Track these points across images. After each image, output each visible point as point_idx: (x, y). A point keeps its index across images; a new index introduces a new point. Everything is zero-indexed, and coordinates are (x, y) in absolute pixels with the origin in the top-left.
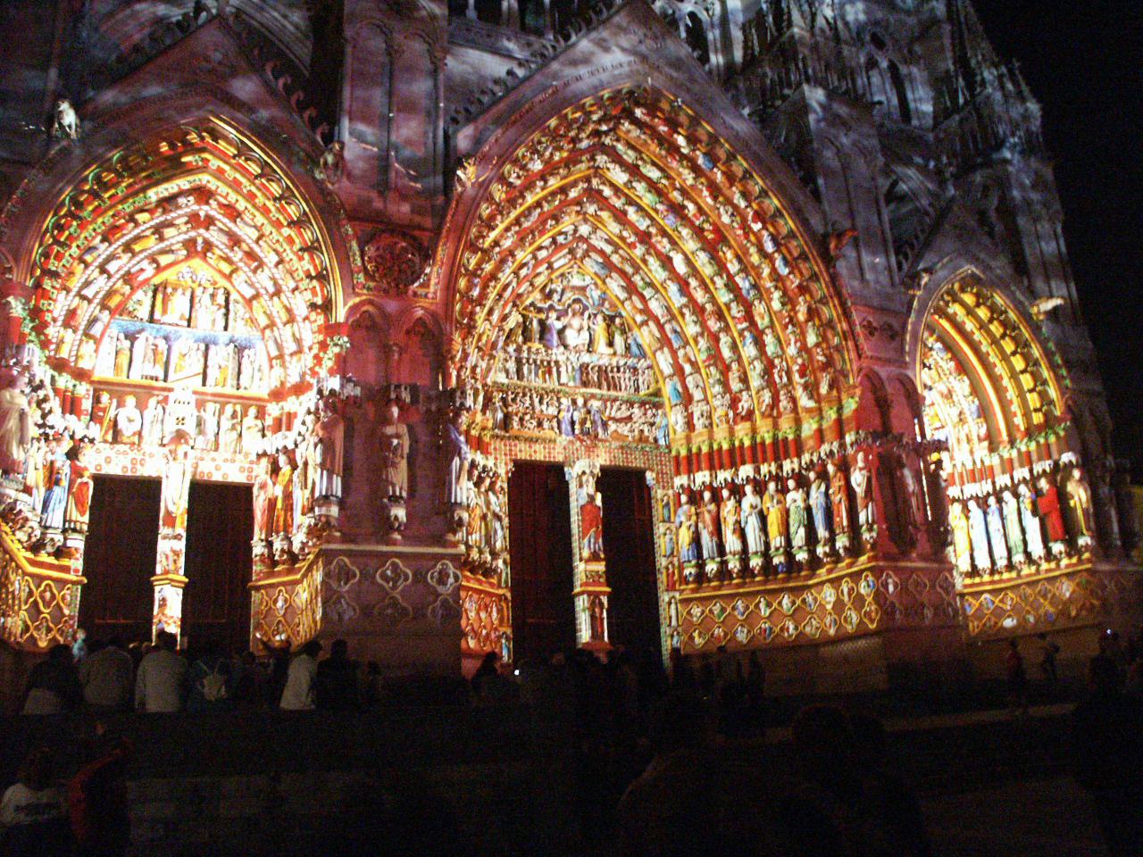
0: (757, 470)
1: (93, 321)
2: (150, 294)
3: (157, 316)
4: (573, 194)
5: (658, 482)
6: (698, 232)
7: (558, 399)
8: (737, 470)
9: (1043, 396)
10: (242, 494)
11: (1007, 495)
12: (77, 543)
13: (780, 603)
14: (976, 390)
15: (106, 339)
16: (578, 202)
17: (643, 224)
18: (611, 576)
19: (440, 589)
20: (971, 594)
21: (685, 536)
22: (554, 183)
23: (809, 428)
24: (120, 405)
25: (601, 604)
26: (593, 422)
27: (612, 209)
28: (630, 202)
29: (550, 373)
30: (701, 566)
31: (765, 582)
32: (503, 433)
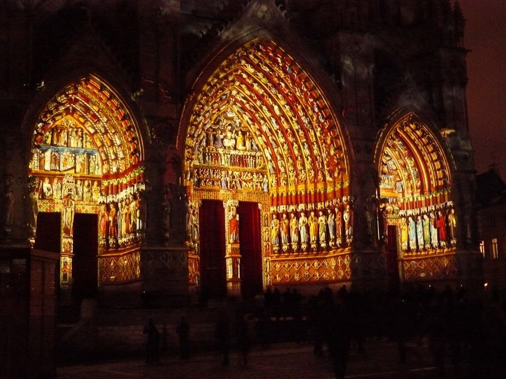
0: (306, 207)
3: (55, 143)
4: (230, 79)
5: (263, 208)
6: (285, 97)
8: (298, 205)
9: (444, 172)
10: (93, 218)
11: (425, 217)
13: (313, 265)
14: (417, 165)
17: (261, 92)
18: (242, 250)
20: (407, 261)
21: (274, 233)
23: (330, 189)
25: (238, 263)
26: (236, 182)
28: (255, 81)
30: (280, 245)
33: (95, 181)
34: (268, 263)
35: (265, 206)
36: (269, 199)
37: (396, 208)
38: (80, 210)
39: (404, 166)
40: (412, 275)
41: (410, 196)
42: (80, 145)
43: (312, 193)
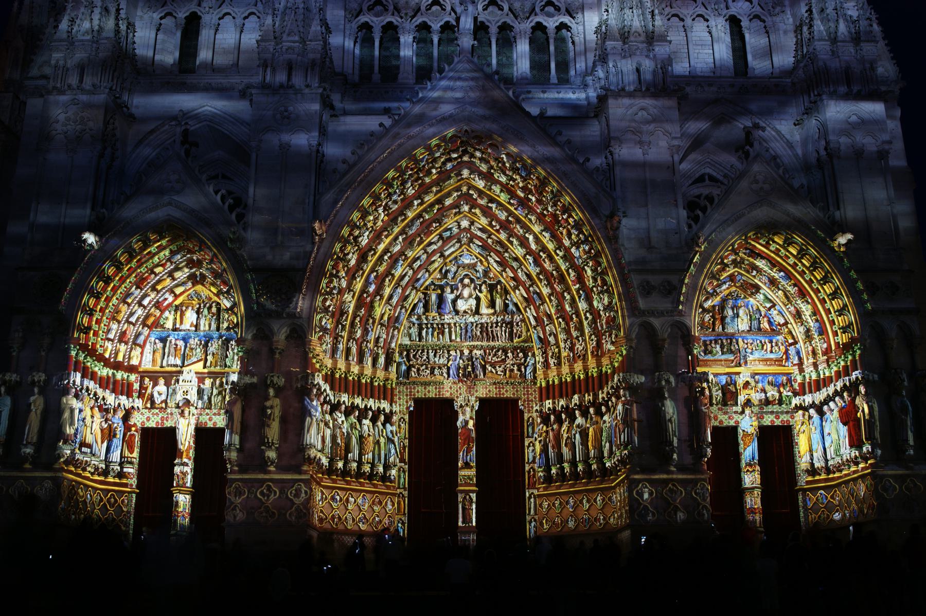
1: (138, 336)
2: (173, 312)
3: (178, 326)
4: (448, 202)
6: (541, 218)
12: (130, 470)
13: (595, 500)
14: (815, 312)
15: (148, 346)
16: (456, 205)
20: (810, 490)
22: (429, 198)
24: (156, 384)
27: (481, 207)
29: (443, 334)
30: (548, 469)
31: (586, 484)
32: (405, 380)
33: (160, 377)
34: (532, 500)
35: (528, 404)
36: (535, 391)
38: (206, 422)
39: (798, 315)
40: (819, 517)
41: (812, 368)
42: (214, 326)
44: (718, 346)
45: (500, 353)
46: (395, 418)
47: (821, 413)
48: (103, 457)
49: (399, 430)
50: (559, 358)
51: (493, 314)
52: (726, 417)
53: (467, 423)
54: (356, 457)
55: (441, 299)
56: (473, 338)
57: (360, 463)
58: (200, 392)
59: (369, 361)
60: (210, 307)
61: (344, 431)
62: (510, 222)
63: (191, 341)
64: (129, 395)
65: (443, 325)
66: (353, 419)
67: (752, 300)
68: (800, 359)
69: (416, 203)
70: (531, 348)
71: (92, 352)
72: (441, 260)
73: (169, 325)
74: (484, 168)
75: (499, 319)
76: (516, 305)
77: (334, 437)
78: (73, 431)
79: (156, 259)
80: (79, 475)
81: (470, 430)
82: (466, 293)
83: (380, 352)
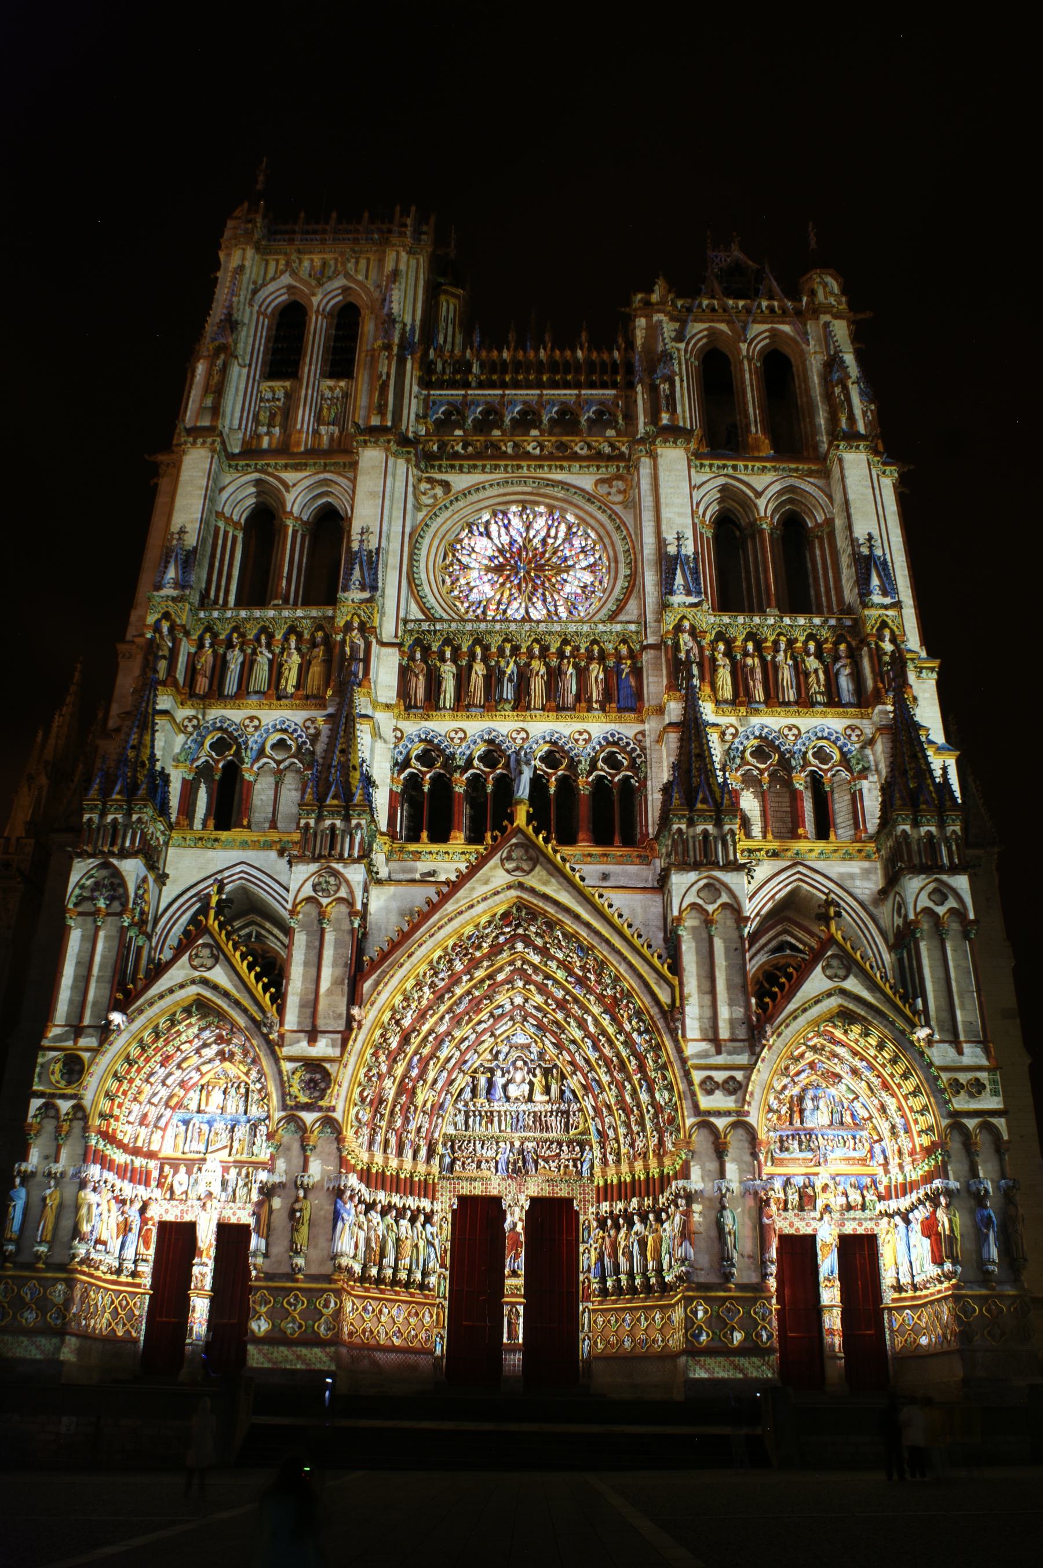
1: (159, 1118)
4: (500, 977)
6: (600, 998)
7: (497, 1143)
12: (146, 1269)
13: (653, 1319)
15: (170, 1127)
16: (509, 981)
19: (325, 1311)
20: (896, 1309)
22: (480, 974)
24: (176, 1173)
25: (518, 1315)
27: (535, 983)
29: (492, 1122)
30: (603, 1280)
31: (645, 1300)
37: (870, 1196)
39: (883, 1109)
41: (897, 1170)
42: (242, 1109)
43: (642, 1177)
44: (796, 1143)
45: (554, 1146)
46: (436, 1218)
47: (907, 1222)
48: (117, 1255)
49: (441, 1232)
50: (618, 1154)
51: (548, 1102)
52: (803, 1224)
53: (515, 1225)
54: (392, 1264)
55: (490, 1083)
56: (525, 1128)
57: (396, 1269)
58: (224, 1184)
59: (409, 1152)
60: (238, 1087)
61: (380, 1233)
62: (567, 1001)
63: (216, 1125)
64: (147, 1184)
65: (492, 1112)
66: (389, 1219)
67: (832, 1091)
68: (886, 1158)
69: (465, 978)
70: (589, 1143)
71: (110, 1138)
72: (492, 1040)
73: (193, 1106)
74: (539, 942)
75: (555, 1108)
76: (573, 1092)
77: (368, 1241)
78: (89, 1229)
79: (183, 1038)
80: (91, 1276)
81: (519, 1234)
82: (519, 1076)
83: (422, 1143)
